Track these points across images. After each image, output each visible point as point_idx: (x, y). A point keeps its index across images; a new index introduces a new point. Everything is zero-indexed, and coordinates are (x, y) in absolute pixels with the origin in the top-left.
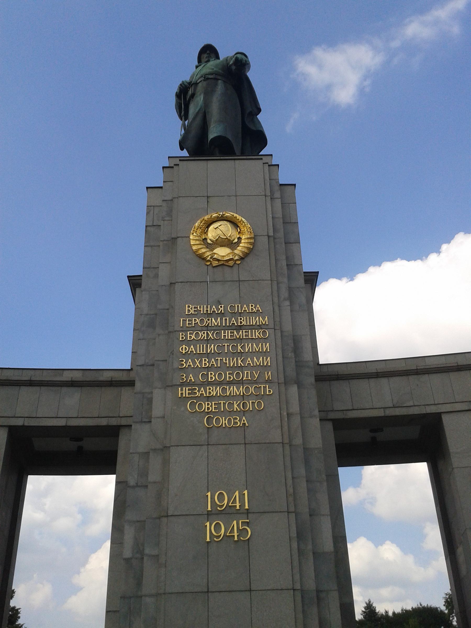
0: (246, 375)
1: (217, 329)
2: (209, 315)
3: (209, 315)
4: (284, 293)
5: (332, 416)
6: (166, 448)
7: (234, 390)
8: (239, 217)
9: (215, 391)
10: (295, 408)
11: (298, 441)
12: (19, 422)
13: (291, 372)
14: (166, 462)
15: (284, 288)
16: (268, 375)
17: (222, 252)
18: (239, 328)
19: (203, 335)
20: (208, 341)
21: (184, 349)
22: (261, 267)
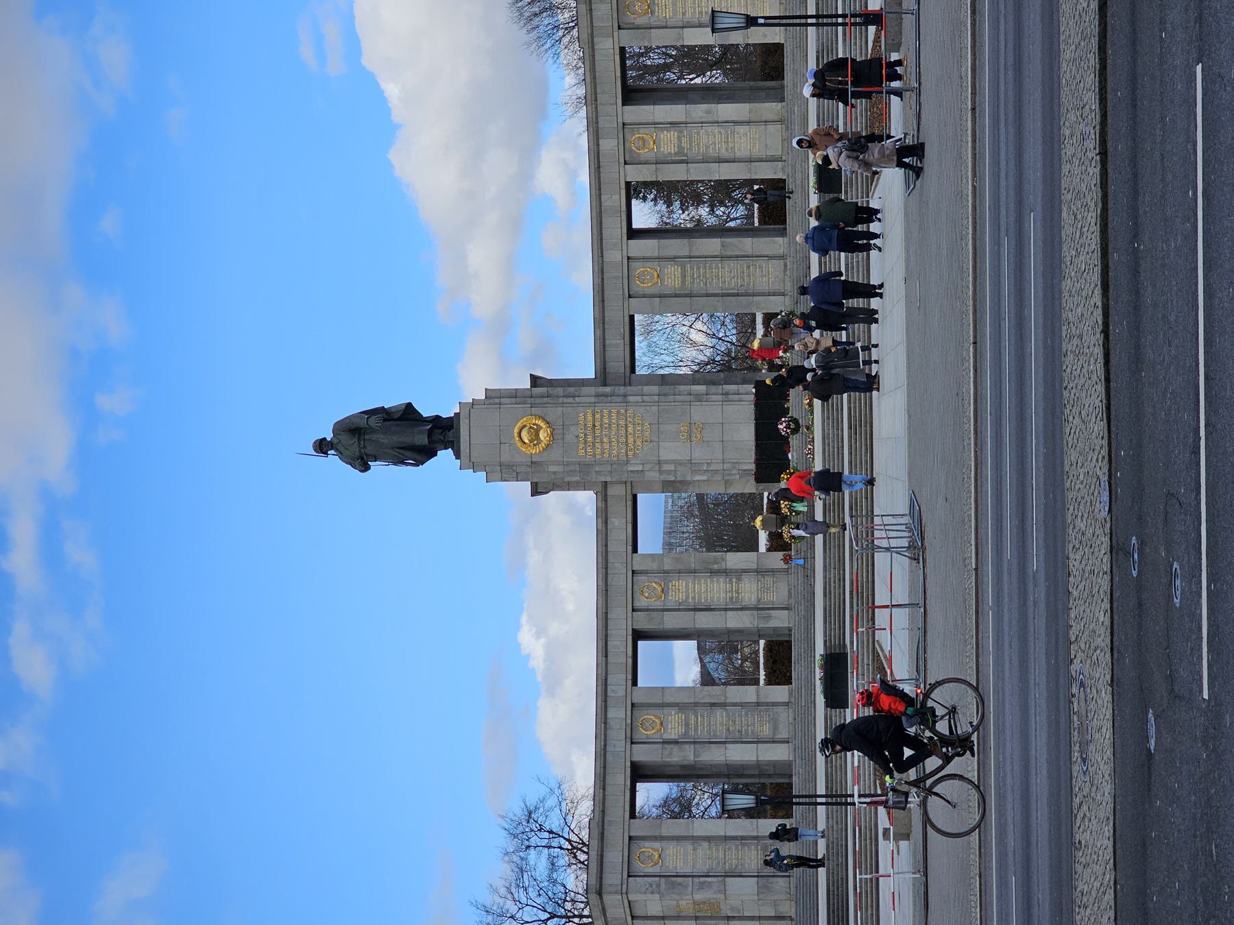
0: (622, 423)
1: (594, 438)
2: (586, 442)
3: (586, 442)
4: (571, 400)
5: (628, 374)
6: (659, 463)
7: (630, 429)
8: (519, 424)
9: (631, 440)
10: (639, 398)
11: (656, 398)
12: (630, 548)
13: (620, 399)
14: (667, 462)
15: (566, 400)
16: (622, 411)
17: (542, 435)
18: (594, 426)
19: (597, 445)
20: (602, 442)
21: (606, 455)
22: (554, 413)
